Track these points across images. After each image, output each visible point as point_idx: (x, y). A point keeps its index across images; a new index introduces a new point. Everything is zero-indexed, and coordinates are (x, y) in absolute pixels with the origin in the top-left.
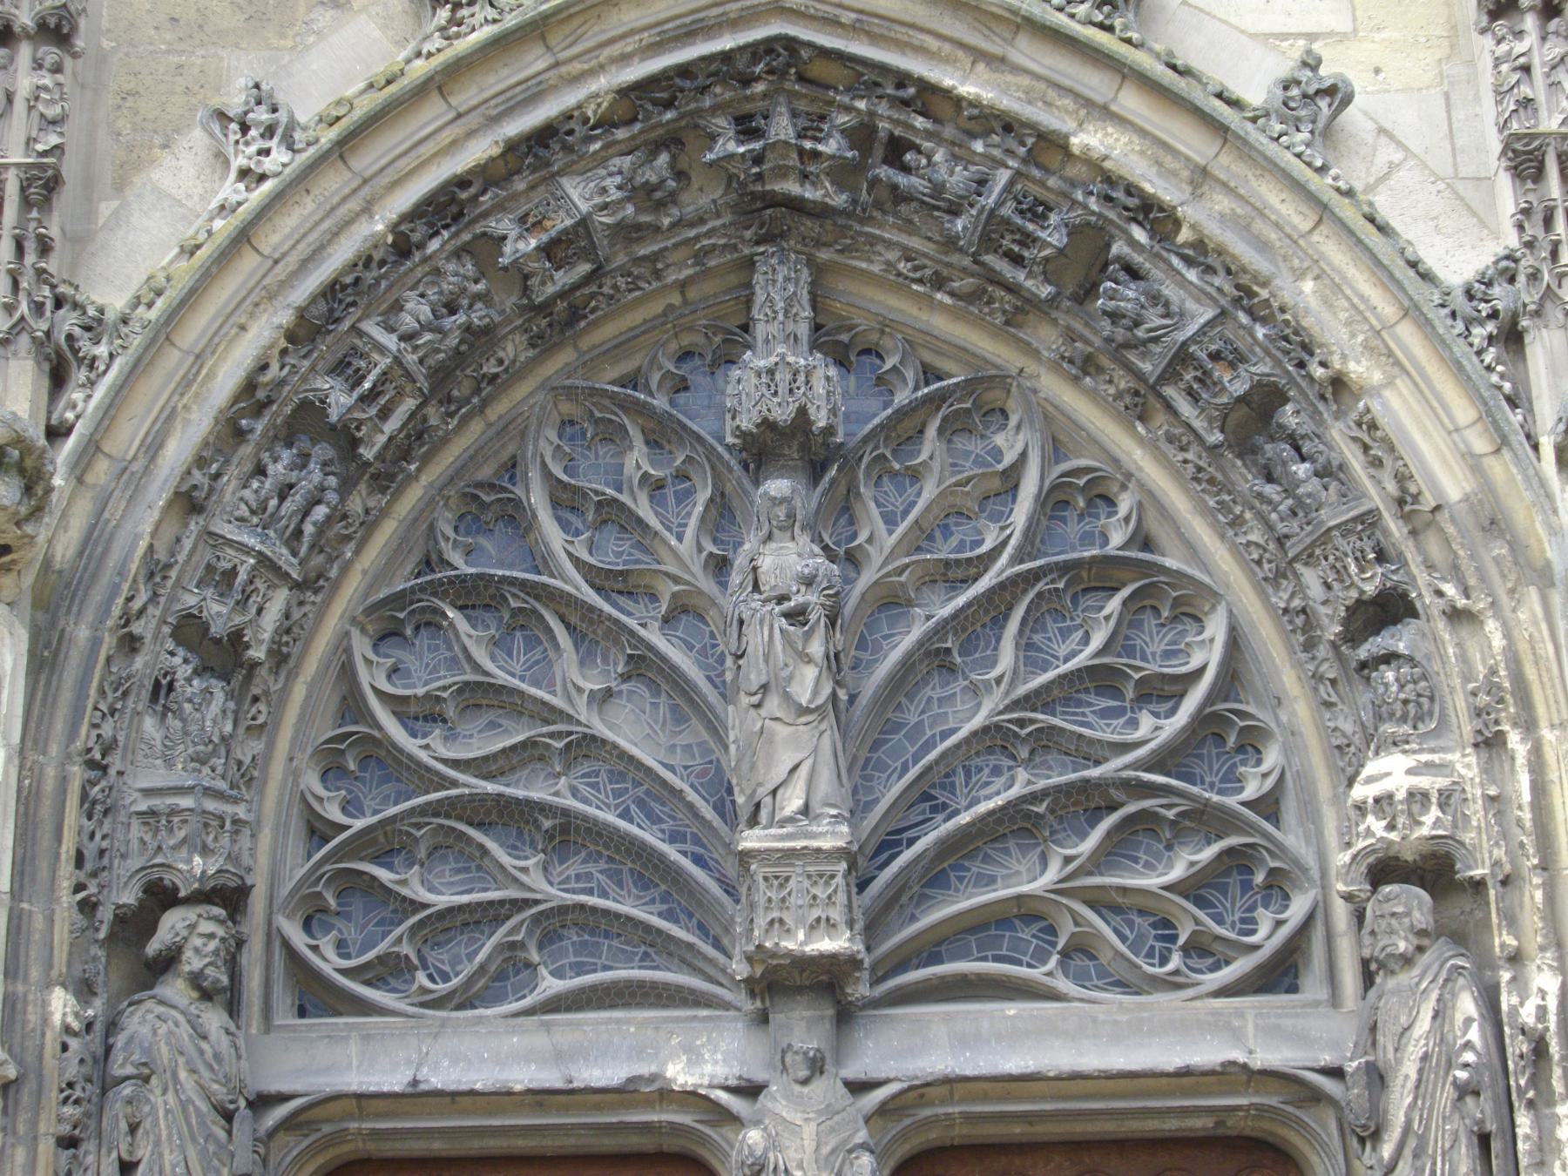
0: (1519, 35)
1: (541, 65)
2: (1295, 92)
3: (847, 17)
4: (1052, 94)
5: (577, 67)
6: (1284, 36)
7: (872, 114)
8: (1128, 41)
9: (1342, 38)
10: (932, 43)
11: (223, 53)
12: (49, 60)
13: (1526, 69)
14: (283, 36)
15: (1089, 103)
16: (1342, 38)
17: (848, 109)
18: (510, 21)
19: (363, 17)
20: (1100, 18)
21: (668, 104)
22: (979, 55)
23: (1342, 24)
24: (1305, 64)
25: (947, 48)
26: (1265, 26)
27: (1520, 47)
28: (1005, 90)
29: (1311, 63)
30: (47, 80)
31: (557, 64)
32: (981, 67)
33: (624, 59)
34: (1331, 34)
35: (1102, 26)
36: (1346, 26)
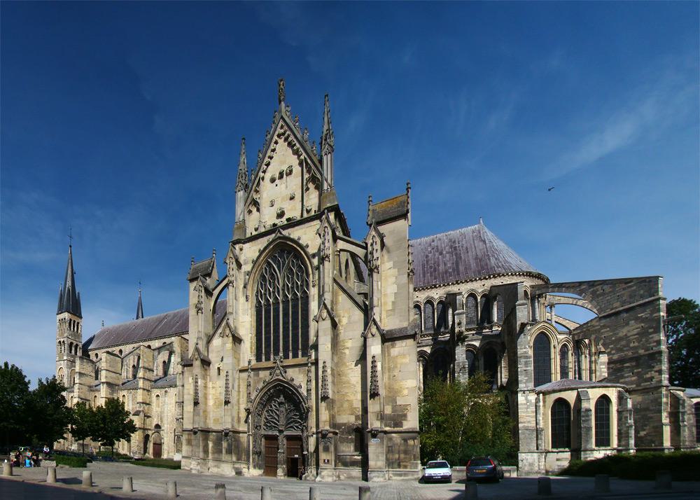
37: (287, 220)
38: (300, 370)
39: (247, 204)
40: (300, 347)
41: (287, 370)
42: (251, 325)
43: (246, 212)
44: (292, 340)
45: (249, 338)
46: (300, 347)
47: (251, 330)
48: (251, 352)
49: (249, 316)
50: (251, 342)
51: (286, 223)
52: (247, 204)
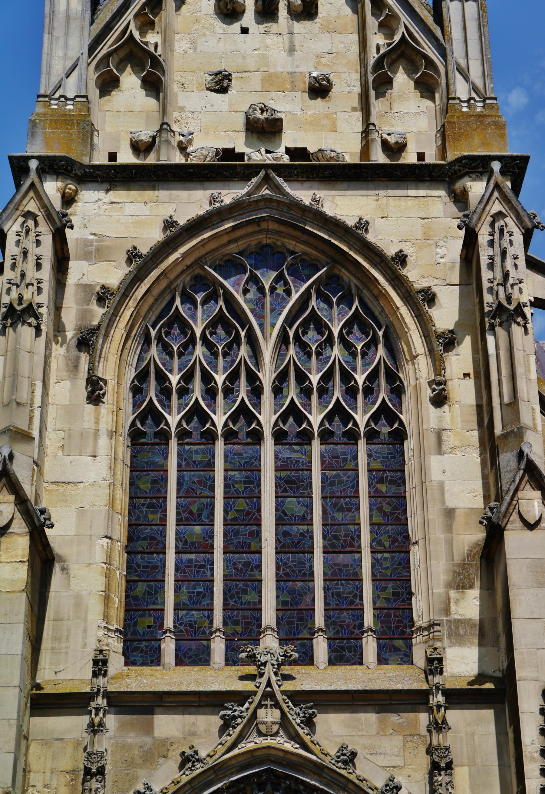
0: (440, 775)
1: (213, 776)
2: (388, 788)
3: (285, 763)
4: (332, 784)
5: (221, 776)
6: (388, 767)
7: (290, 784)
8: (350, 773)
9: (401, 767)
10: (305, 770)
11: (138, 770)
12: (100, 780)
13: (441, 785)
14: (152, 765)
15: (340, 787)
16: (401, 767)
17: (285, 783)
18: (206, 767)
19: (171, 760)
20: (343, 767)
21: (241, 783)
22: (315, 774)
23: (402, 764)
24: (391, 780)
25: (308, 771)
26: (383, 765)
27: (440, 778)
28: (321, 783)
29: (392, 779)
30: (99, 786)
31: (217, 776)
32: (316, 776)
33: (232, 775)
34: (399, 766)
35: (344, 769)
36: (402, 764)
37: (288, 151)
38: (380, 721)
39: (104, 50)
40: (369, 620)
41: (321, 719)
42: (112, 503)
43: (93, 76)
44: (326, 589)
45: (100, 556)
46: (369, 620)
47: (110, 519)
48: (106, 617)
49: (103, 462)
50: (108, 575)
51: (286, 159)
52: (104, 50)
